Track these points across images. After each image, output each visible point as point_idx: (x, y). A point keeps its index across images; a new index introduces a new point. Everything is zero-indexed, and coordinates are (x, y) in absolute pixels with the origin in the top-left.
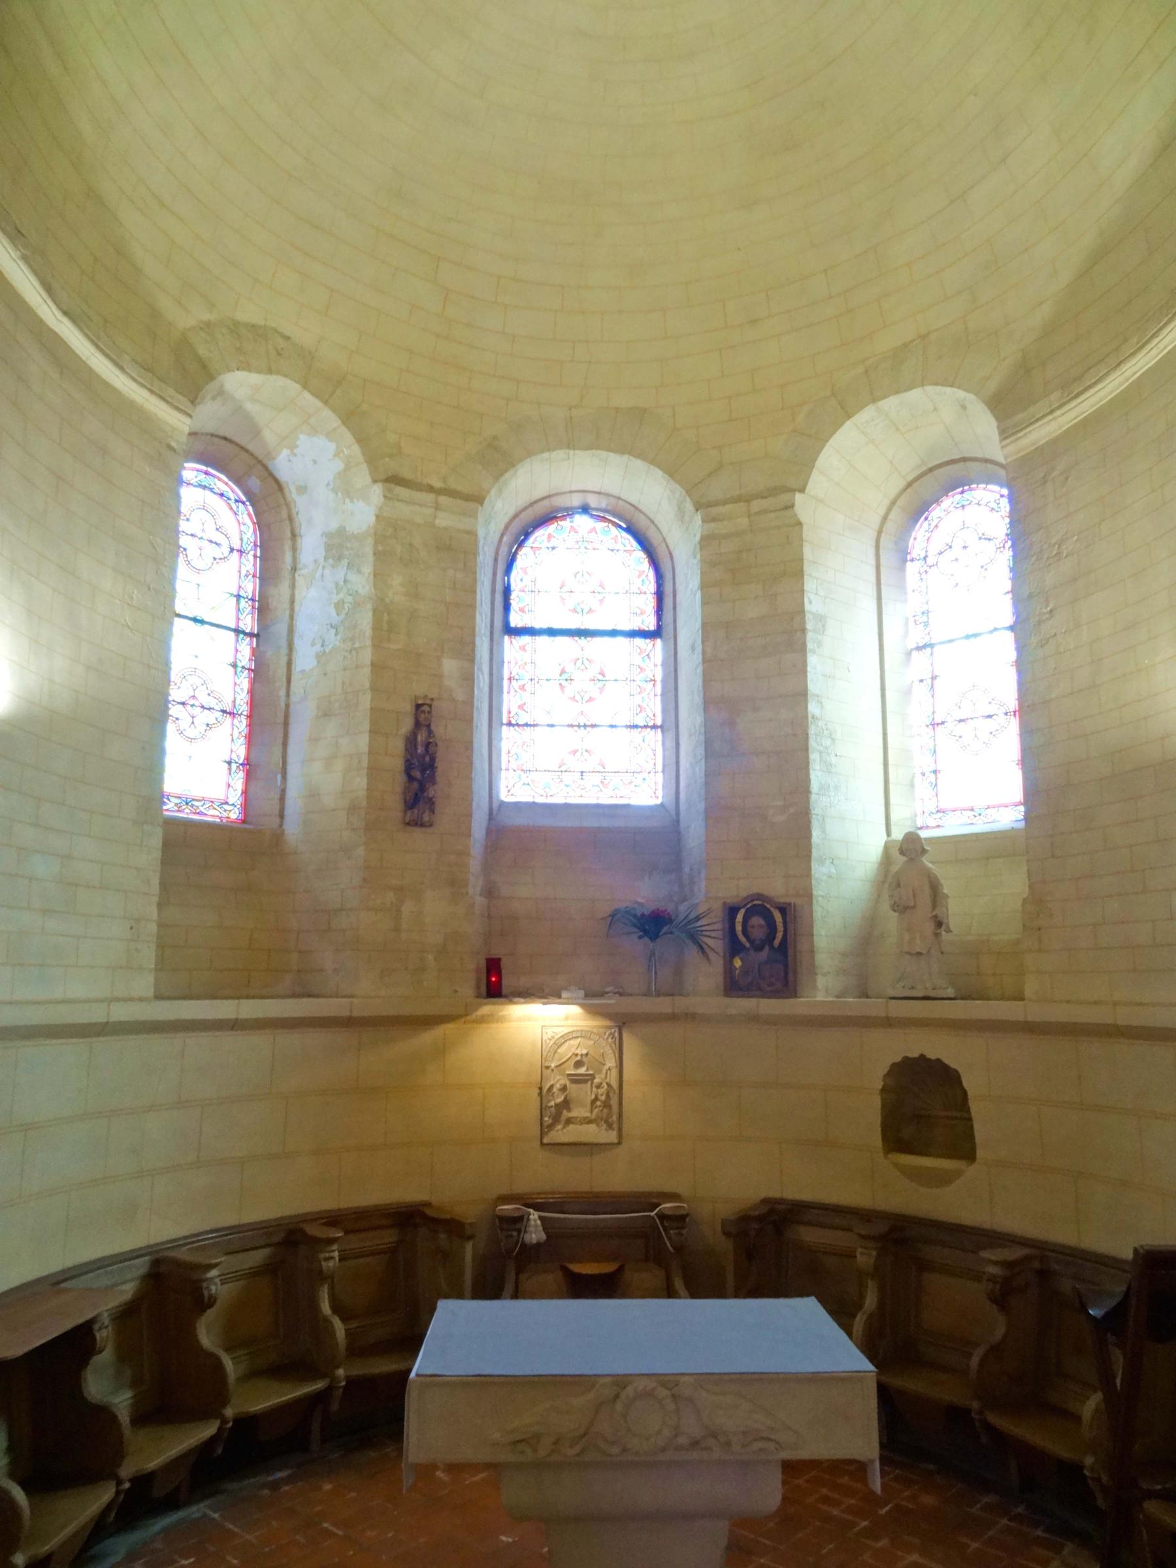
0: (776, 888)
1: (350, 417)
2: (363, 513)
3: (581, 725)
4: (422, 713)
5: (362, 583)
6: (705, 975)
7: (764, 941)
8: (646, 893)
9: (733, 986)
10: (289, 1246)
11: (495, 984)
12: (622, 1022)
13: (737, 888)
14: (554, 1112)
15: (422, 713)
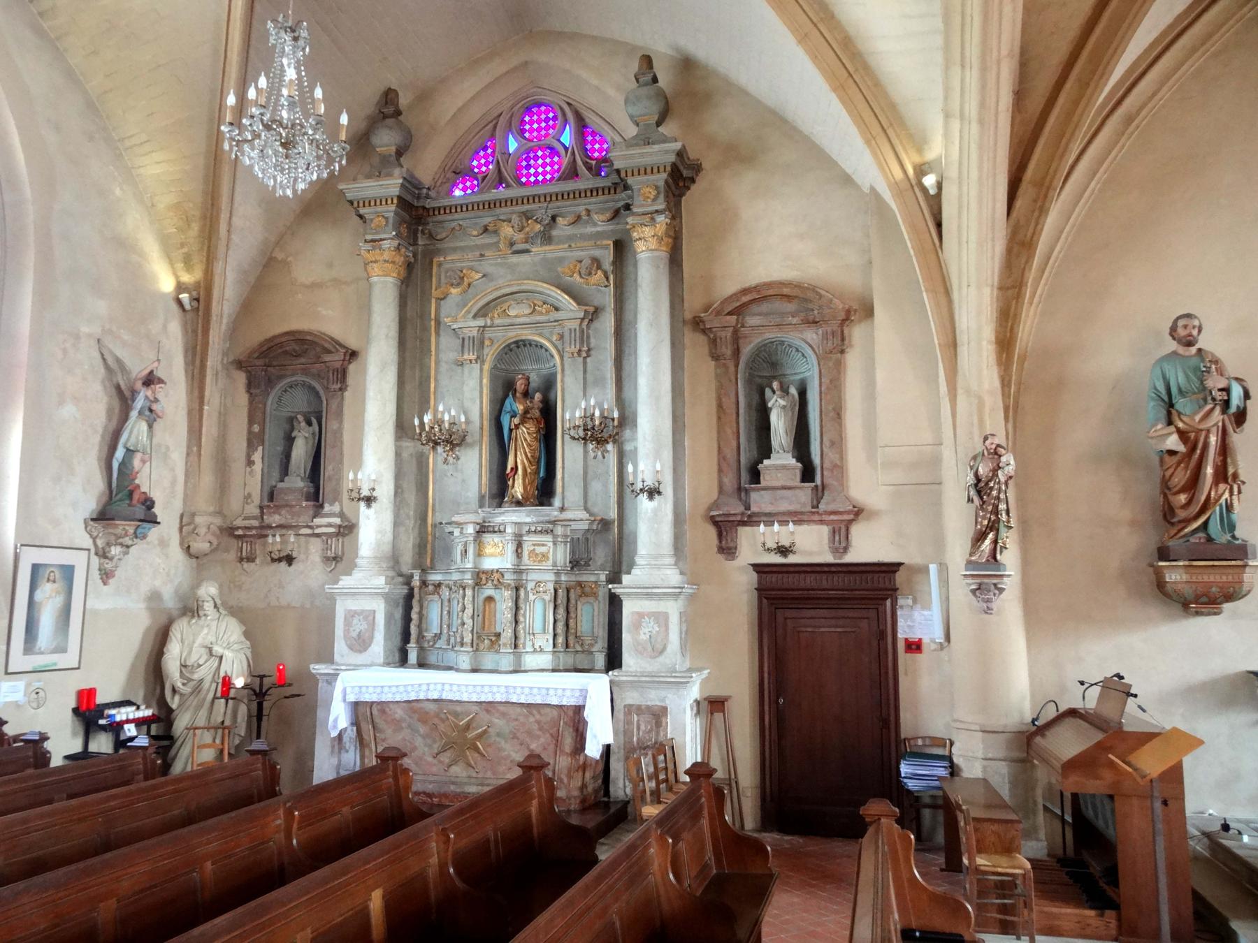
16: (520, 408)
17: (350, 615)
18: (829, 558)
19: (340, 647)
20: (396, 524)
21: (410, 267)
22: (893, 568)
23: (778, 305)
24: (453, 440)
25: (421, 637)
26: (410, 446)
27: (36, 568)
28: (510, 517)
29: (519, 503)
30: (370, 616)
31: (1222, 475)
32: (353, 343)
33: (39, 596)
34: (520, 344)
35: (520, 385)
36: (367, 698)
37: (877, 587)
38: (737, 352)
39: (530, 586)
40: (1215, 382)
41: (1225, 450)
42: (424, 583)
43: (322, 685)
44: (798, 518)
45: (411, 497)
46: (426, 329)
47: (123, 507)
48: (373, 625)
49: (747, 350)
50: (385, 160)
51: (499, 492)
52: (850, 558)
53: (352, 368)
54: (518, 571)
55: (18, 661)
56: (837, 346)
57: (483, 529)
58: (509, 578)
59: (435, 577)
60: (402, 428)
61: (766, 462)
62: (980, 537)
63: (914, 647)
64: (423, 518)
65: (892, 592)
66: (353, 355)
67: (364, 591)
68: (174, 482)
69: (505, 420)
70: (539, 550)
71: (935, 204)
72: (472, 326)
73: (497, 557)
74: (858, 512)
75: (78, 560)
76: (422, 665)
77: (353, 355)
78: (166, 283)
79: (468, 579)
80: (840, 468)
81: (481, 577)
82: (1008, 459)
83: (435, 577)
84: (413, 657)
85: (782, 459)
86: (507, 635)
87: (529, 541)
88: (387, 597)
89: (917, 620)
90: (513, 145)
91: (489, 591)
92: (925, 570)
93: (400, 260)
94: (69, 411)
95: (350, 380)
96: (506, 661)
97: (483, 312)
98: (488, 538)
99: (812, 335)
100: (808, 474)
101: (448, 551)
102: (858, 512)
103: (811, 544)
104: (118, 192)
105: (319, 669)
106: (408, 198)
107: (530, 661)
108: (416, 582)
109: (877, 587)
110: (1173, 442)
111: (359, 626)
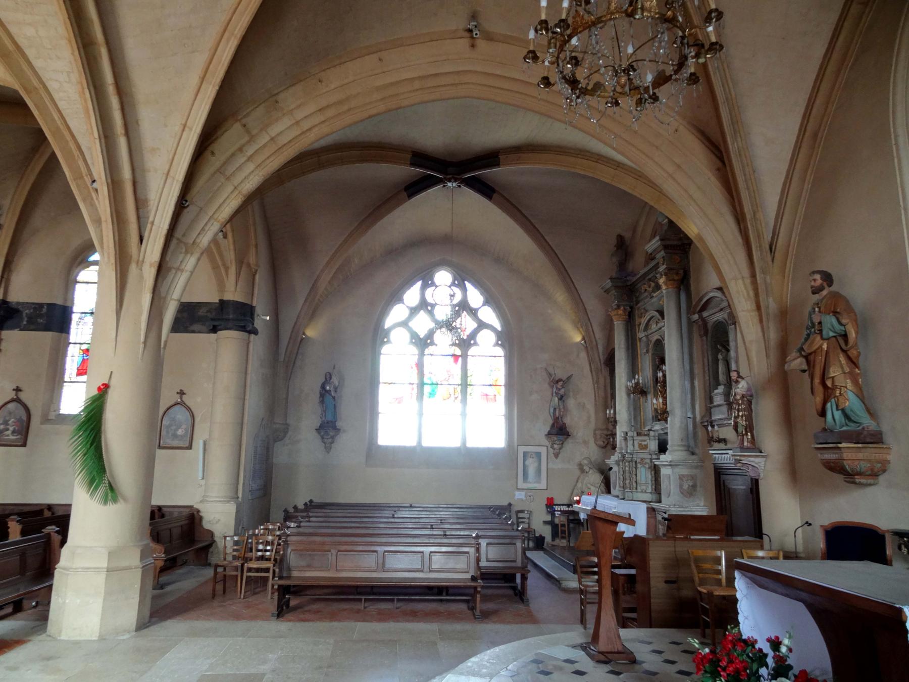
27: (525, 454)
33: (527, 463)
34: (658, 340)
39: (639, 460)
47: (560, 431)
55: (521, 484)
61: (716, 391)
68: (589, 418)
70: (644, 443)
75: (543, 450)
78: (578, 338)
93: (620, 312)
94: (535, 397)
97: (646, 329)
104: (550, 311)
106: (620, 284)
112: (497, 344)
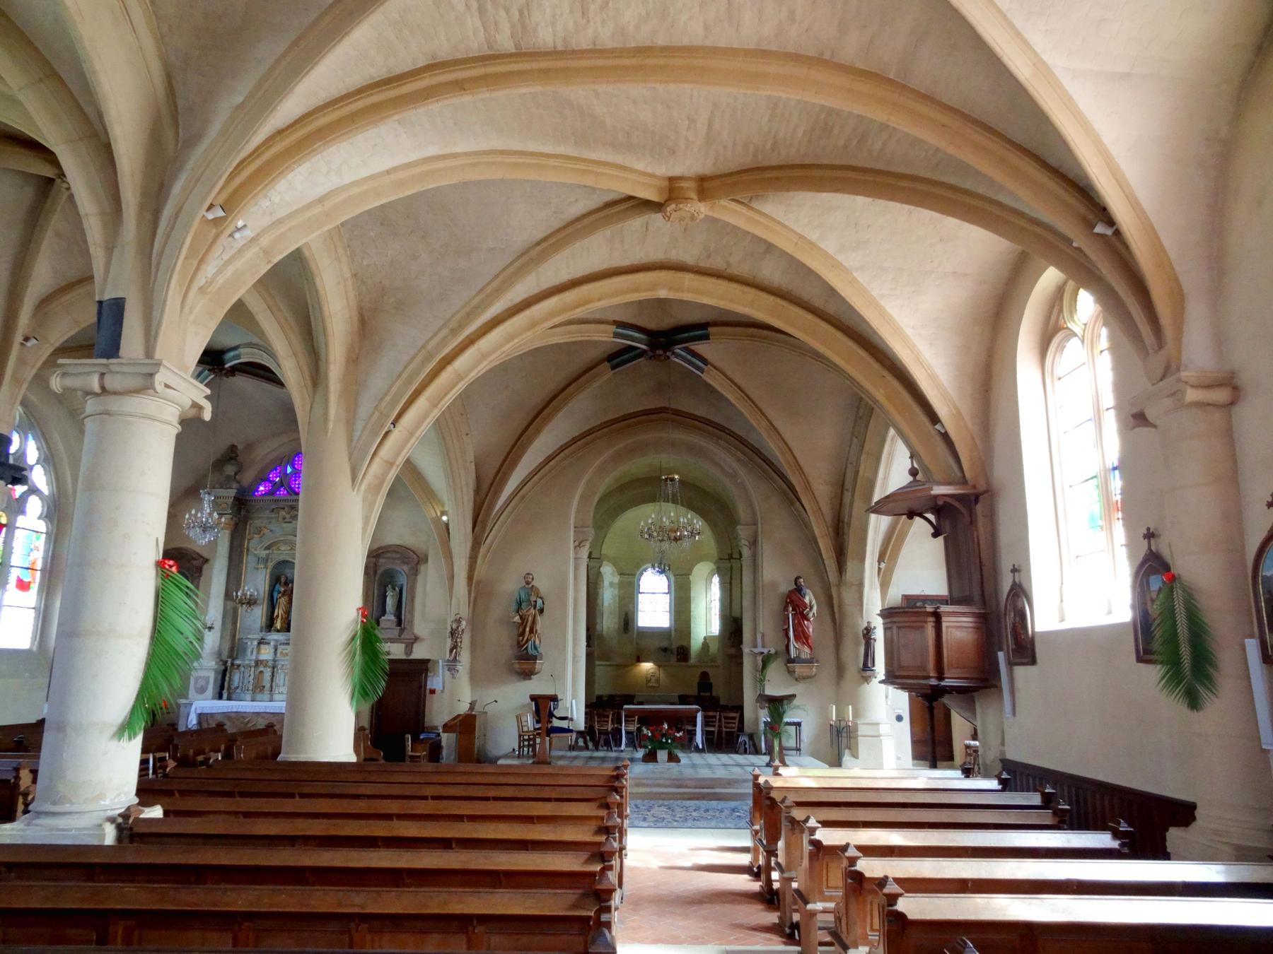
0: (685, 644)
1: (614, 564)
2: (616, 579)
3: (654, 609)
4: (626, 615)
5: (616, 592)
6: (674, 658)
7: (683, 653)
8: (665, 644)
9: (678, 660)
10: (611, 697)
11: (639, 660)
12: (659, 666)
13: (679, 644)
14: (648, 681)
15: (626, 615)
16: (282, 589)
17: (197, 679)
18: (404, 657)
19: (192, 692)
20: (222, 638)
21: (236, 525)
22: (428, 661)
23: (394, 555)
24: (251, 602)
25: (229, 688)
26: (230, 603)
28: (273, 636)
29: (278, 631)
30: (207, 679)
31: (531, 631)
32: (206, 555)
35: (283, 579)
36: (206, 711)
37: (421, 668)
38: (375, 573)
40: (533, 599)
41: (534, 622)
42: (233, 664)
43: (182, 709)
44: (392, 641)
45: (229, 626)
46: (242, 552)
48: (207, 683)
49: (379, 572)
50: (228, 478)
51: (270, 625)
52: (413, 657)
53: (205, 567)
54: (275, 661)
56: (415, 572)
57: (261, 642)
58: (270, 663)
59: (237, 662)
60: (228, 596)
62: (451, 651)
63: (433, 692)
64: (234, 636)
65: (427, 670)
66: (206, 561)
67: (206, 669)
69: (275, 595)
71: (447, 525)
72: (263, 553)
73: (266, 654)
74: (416, 639)
76: (229, 699)
77: (206, 561)
79: (253, 663)
80: (411, 622)
81: (258, 663)
82: (464, 623)
83: (237, 662)
84: (225, 696)
85: (390, 617)
86: (268, 686)
87: (280, 648)
88: (215, 671)
89: (436, 681)
90: (289, 470)
91: (261, 669)
92: (436, 662)
95: (204, 572)
96: (266, 695)
97: (268, 548)
98: (262, 646)
99: (405, 568)
100: (399, 623)
101: (245, 650)
102: (416, 639)
103: (396, 651)
105: (183, 701)
107: (276, 697)
108: (229, 664)
109: (421, 668)
110: (517, 619)
111: (201, 683)
112: (40, 518)
